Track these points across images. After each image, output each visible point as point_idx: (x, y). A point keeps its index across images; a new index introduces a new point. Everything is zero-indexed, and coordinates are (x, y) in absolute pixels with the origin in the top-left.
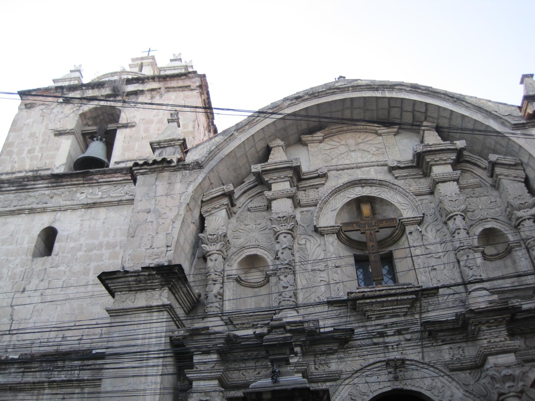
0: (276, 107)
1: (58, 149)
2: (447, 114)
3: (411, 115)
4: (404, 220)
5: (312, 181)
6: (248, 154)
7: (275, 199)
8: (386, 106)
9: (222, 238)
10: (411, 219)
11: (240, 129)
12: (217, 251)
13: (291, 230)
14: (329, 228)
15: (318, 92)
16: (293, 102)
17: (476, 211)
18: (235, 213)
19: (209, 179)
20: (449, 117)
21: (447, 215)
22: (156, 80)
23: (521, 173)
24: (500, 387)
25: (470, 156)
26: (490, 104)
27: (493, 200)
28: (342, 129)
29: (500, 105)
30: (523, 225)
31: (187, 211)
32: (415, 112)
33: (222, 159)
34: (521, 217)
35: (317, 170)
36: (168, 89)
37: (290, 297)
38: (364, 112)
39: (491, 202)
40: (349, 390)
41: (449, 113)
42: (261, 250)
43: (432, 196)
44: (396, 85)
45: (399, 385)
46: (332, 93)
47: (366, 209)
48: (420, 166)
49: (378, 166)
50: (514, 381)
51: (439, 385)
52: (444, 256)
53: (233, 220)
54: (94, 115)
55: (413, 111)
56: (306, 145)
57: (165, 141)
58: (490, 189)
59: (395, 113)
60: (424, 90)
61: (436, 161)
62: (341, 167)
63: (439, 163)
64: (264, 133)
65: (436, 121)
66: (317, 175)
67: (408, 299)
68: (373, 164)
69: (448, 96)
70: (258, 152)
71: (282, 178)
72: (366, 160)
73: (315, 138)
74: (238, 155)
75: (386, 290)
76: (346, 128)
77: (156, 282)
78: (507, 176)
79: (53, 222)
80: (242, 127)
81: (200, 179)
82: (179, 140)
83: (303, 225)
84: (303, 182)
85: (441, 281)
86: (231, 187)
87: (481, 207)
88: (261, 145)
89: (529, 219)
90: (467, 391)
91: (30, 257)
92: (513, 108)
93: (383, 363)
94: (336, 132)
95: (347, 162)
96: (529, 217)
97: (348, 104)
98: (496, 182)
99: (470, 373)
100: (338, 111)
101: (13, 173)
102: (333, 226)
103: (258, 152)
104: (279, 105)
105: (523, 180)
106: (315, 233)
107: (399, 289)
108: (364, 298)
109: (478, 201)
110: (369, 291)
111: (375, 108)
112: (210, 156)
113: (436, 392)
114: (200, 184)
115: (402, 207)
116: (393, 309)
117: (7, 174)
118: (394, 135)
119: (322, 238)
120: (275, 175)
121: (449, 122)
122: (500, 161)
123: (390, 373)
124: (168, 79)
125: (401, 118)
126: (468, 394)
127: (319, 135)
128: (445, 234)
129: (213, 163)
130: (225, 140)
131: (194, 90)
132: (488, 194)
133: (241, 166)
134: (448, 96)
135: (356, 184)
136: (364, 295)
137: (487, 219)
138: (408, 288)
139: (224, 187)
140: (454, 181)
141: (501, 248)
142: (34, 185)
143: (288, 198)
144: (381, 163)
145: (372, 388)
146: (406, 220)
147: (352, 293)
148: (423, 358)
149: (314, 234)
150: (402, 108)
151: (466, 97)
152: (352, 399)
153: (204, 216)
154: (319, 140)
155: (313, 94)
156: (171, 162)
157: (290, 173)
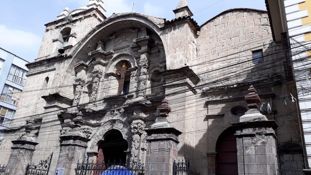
1: (53, 47)
5: (109, 55)
26: (155, 19)
36: (85, 17)
37: (92, 99)
44: (129, 14)
55: (138, 23)
57: (67, 47)
59: (133, 24)
62: (118, 49)
66: (109, 53)
72: (126, 45)
73: (113, 37)
79: (48, 75)
81: (71, 62)
82: (70, 46)
84: (107, 56)
86: (82, 62)
88: (94, 44)
89: (163, 67)
95: (121, 46)
97: (117, 24)
101: (41, 58)
103: (94, 46)
114: (71, 63)
120: (96, 56)
127: (114, 37)
129: (75, 55)
130: (79, 46)
131: (92, 16)
139: (80, 62)
151: (149, 17)
156: (64, 56)
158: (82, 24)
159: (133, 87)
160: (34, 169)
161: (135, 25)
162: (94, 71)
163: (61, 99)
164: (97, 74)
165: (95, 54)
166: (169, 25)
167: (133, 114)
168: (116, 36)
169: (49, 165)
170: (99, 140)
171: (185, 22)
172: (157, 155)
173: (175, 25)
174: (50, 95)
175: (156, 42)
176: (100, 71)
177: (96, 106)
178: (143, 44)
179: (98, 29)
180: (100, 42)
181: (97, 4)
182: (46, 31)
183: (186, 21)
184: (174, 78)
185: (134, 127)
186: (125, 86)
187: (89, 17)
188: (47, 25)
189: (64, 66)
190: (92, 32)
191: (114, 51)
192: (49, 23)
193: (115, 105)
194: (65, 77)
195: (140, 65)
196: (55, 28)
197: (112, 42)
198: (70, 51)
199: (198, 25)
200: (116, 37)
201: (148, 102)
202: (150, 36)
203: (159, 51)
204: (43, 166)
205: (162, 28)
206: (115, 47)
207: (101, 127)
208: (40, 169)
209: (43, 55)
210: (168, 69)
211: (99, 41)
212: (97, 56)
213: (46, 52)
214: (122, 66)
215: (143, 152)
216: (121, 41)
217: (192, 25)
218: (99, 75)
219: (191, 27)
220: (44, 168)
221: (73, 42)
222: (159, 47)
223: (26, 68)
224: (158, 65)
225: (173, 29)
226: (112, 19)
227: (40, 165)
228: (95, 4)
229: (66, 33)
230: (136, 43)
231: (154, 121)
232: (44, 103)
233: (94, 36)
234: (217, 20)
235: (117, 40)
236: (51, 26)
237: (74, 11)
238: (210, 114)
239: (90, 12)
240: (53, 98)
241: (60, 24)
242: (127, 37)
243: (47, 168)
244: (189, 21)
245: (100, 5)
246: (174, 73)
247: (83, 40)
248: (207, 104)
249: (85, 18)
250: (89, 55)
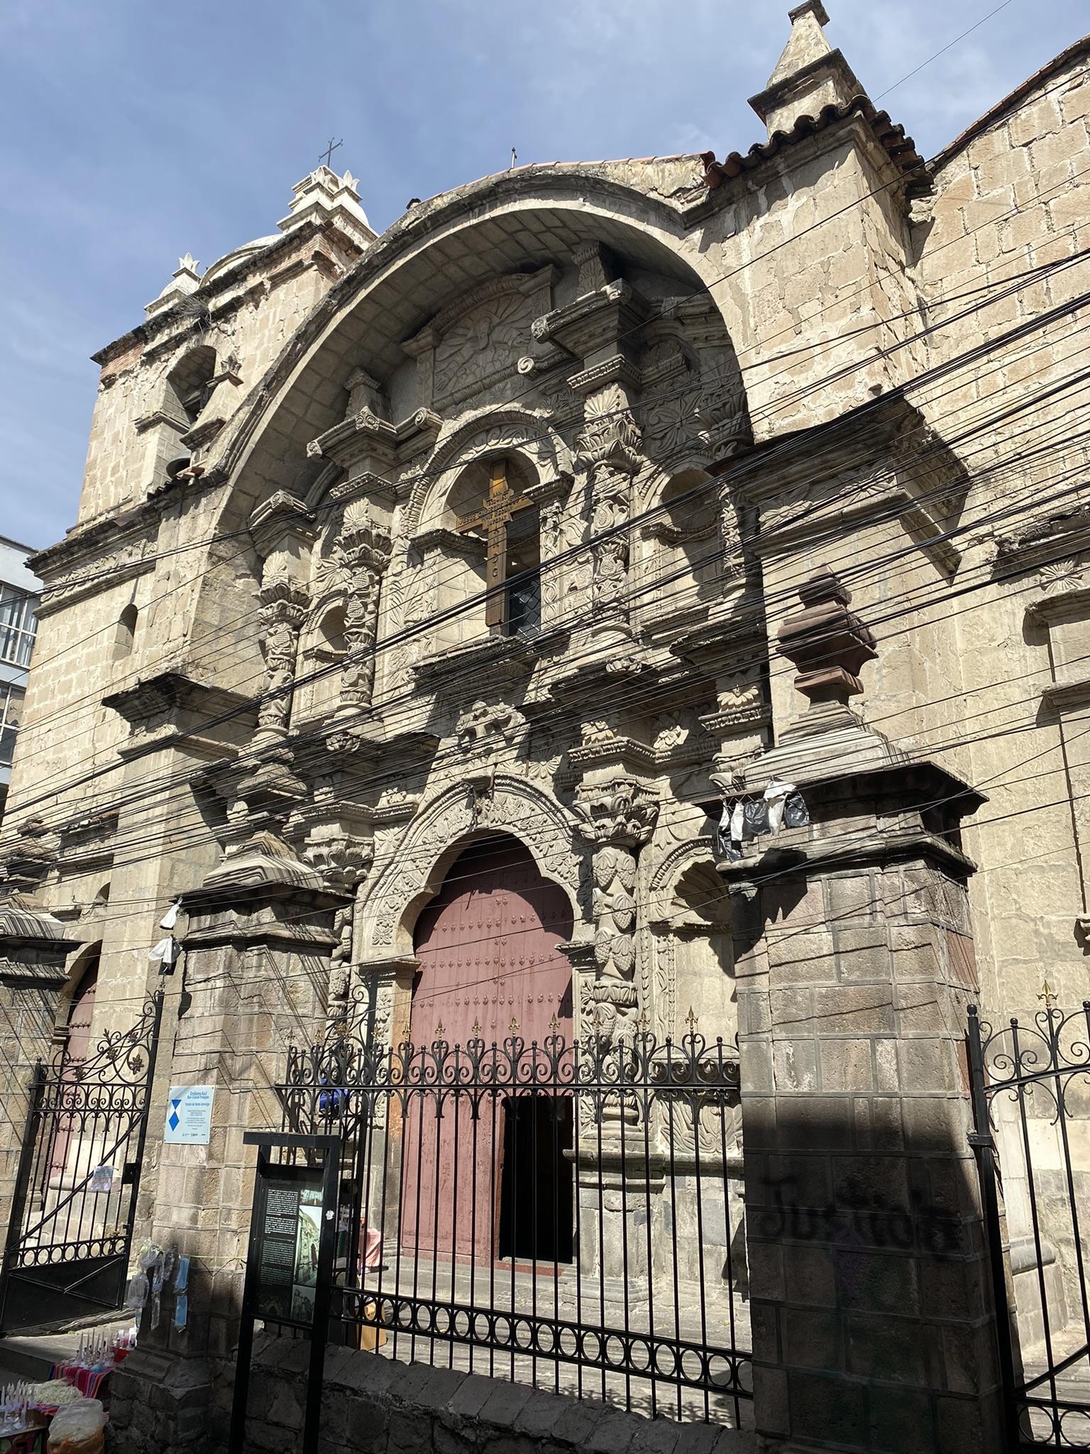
1: (143, 457)
5: (415, 441)
6: (309, 417)
8: (504, 236)
22: (260, 265)
36: (276, 281)
44: (497, 184)
54: (193, 367)
55: (549, 229)
63: (591, 344)
70: (331, 407)
72: (498, 366)
73: (423, 342)
76: (469, 301)
77: (161, 700)
82: (213, 424)
84: (403, 447)
89: (726, 444)
91: (110, 662)
92: (693, 162)
95: (470, 379)
97: (438, 257)
101: (94, 519)
103: (331, 407)
109: (677, 407)
111: (489, 245)
117: (87, 522)
124: (275, 256)
125: (548, 248)
127: (426, 337)
129: (241, 464)
130: (253, 413)
139: (271, 499)
140: (613, 382)
142: (106, 538)
150: (525, 229)
156: (186, 479)
158: (267, 317)
159: (563, 595)
160: (72, 1083)
161: (539, 245)
162: (345, 534)
163: (196, 695)
164: (370, 553)
165: (341, 441)
166: (739, 186)
167: (577, 738)
168: (437, 330)
169: (153, 1055)
170: (413, 894)
171: (838, 140)
172: (829, 977)
173: (777, 176)
174: (142, 685)
175: (669, 304)
176: (374, 532)
177: (381, 720)
178: (592, 336)
179: (341, 306)
180: (360, 376)
181: (328, 205)
182: (102, 386)
183: (841, 133)
184: (813, 483)
185: (592, 807)
186: (517, 592)
187: (295, 276)
188: (102, 358)
189: (193, 529)
190: (313, 327)
191: (439, 411)
192: (113, 347)
193: (473, 701)
194: (205, 584)
195: (589, 455)
196: (143, 364)
197: (423, 367)
198: (213, 451)
199: (919, 151)
200: (440, 337)
201: (661, 657)
202: (627, 280)
203: (689, 364)
204: (118, 1063)
205: (698, 207)
206: (442, 388)
208: (105, 1079)
209: (100, 502)
210: (762, 432)
211: (351, 373)
212: (352, 456)
213: (112, 488)
214: (486, 490)
215: (663, 945)
216: (467, 351)
217: (880, 158)
218: (377, 553)
219: (871, 169)
220: (131, 1078)
221: (225, 402)
222: (686, 333)
223: (32, 582)
224: (690, 443)
225: (762, 200)
226: (405, 233)
227: (105, 1060)
228: (317, 206)
229: (194, 380)
230: (549, 337)
231: (705, 766)
232: (118, 730)
233: (322, 347)
234: (1034, 109)
235: (444, 352)
236: (122, 359)
237: (220, 265)
238: (1066, 678)
239: (298, 249)
240: (159, 700)
241: (161, 338)
242: (499, 324)
243: (144, 1070)
244: (866, 130)
245: (341, 210)
246: (807, 454)
247: (273, 381)
248: (1038, 625)
249: (274, 286)
250: (310, 454)
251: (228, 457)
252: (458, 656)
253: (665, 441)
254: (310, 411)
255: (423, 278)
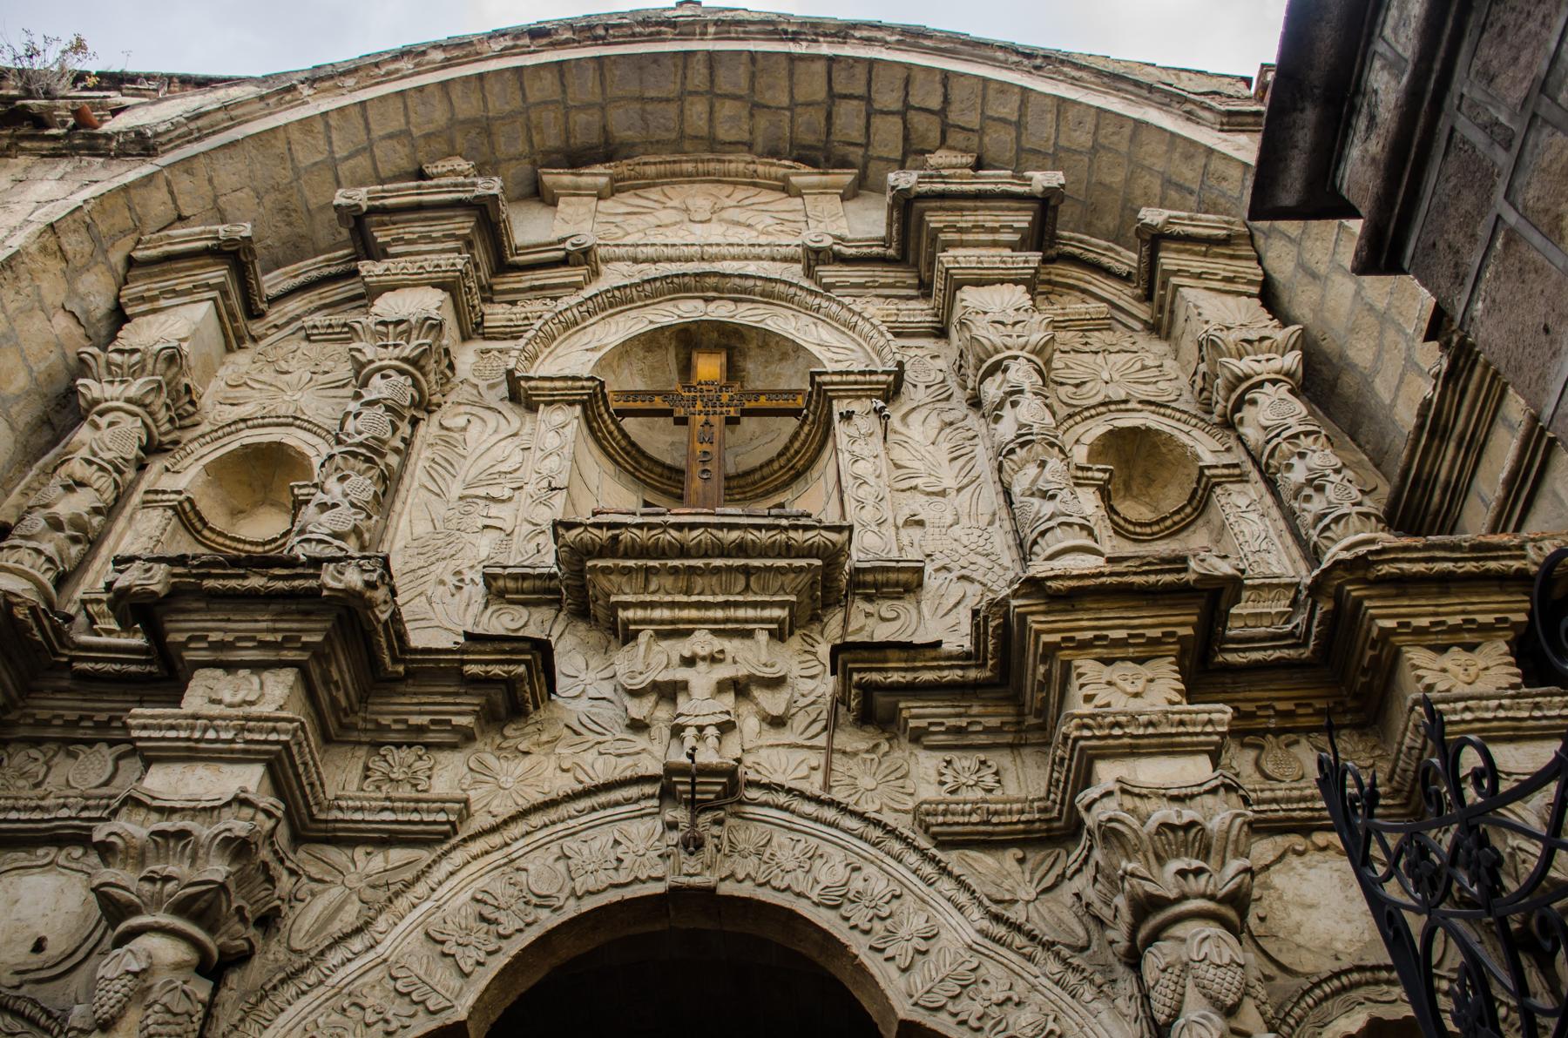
0: (459, 46)
2: (1009, 110)
3: (895, 124)
4: (826, 378)
7: (393, 288)
8: (821, 95)
9: (161, 366)
10: (852, 378)
11: (322, 79)
12: (129, 400)
13: (414, 362)
14: (559, 384)
15: (607, 27)
16: (519, 43)
17: (1089, 386)
18: (255, 340)
19: (171, 193)
20: (1014, 118)
21: (982, 361)
23: (1252, 270)
24: (1143, 872)
25: (1081, 241)
27: (1148, 362)
28: (677, 167)
29: (1183, 75)
30: (1253, 402)
31: (43, 249)
32: (911, 114)
33: (233, 144)
34: (1248, 377)
35: (563, 240)
38: (752, 116)
39: (1144, 368)
40: (479, 884)
41: (1015, 100)
42: (300, 433)
43: (942, 343)
45: (695, 872)
46: (651, 34)
47: (709, 367)
48: (911, 258)
49: (773, 259)
50: (1205, 853)
51: (880, 886)
52: (959, 490)
53: (242, 359)
56: (553, 203)
58: (1142, 340)
60: (942, 40)
61: (961, 230)
62: (650, 251)
64: (407, 116)
65: (975, 139)
67: (791, 569)
68: (758, 250)
69: (1018, 53)
71: (434, 241)
74: (305, 158)
75: (706, 525)
76: (689, 167)
78: (1199, 276)
80: (331, 77)
83: (475, 381)
85: (938, 555)
87: (1106, 377)
90: (997, 918)
93: (648, 789)
94: (659, 176)
96: (1273, 376)
98: (1161, 309)
99: (1021, 861)
100: (668, 100)
102: (574, 379)
104: (471, 43)
105: (1255, 290)
106: (510, 404)
107: (758, 527)
108: (612, 548)
110: (640, 526)
111: (784, 100)
112: (192, 126)
113: (860, 916)
115: (830, 355)
116: (726, 605)
118: (844, 198)
119: (529, 417)
121: (1018, 138)
122: (1177, 229)
123: (672, 826)
126: (1000, 930)
127: (597, 176)
128: (971, 434)
132: (1134, 348)
133: (312, 207)
134: (1018, 53)
135: (687, 289)
136: (615, 538)
137: (1126, 402)
138: (795, 528)
139: (221, 228)
140: (1016, 283)
141: (1173, 498)
143: (434, 286)
144: (783, 250)
145: (579, 881)
146: (836, 378)
147: (570, 526)
148: (827, 786)
149: (506, 407)
150: (868, 99)
152: (483, 918)
153: (128, 311)
154: (595, 187)
155: (590, 28)
157: (464, 225)
165: (419, 207)
168: (614, 179)
178: (979, 227)
190: (438, 56)
200: (615, 188)
207: (458, 857)
233: (444, 85)
251: (176, 126)
252: (693, 526)
253: (1079, 391)
254: (352, 162)
255: (652, 93)
